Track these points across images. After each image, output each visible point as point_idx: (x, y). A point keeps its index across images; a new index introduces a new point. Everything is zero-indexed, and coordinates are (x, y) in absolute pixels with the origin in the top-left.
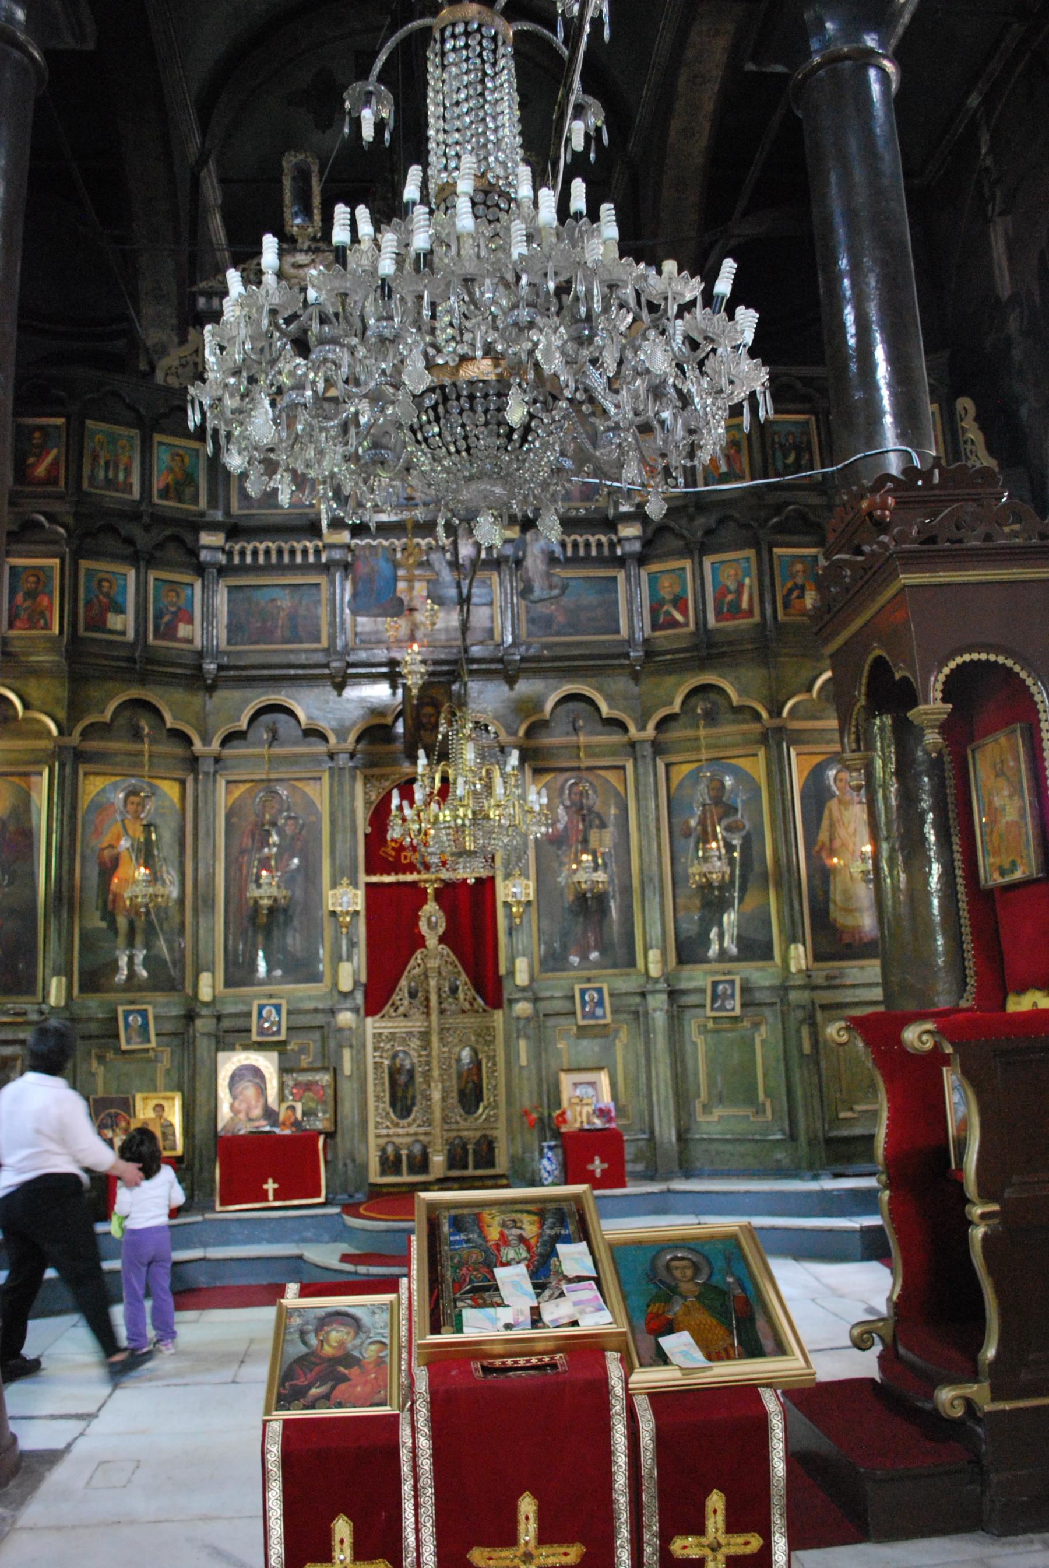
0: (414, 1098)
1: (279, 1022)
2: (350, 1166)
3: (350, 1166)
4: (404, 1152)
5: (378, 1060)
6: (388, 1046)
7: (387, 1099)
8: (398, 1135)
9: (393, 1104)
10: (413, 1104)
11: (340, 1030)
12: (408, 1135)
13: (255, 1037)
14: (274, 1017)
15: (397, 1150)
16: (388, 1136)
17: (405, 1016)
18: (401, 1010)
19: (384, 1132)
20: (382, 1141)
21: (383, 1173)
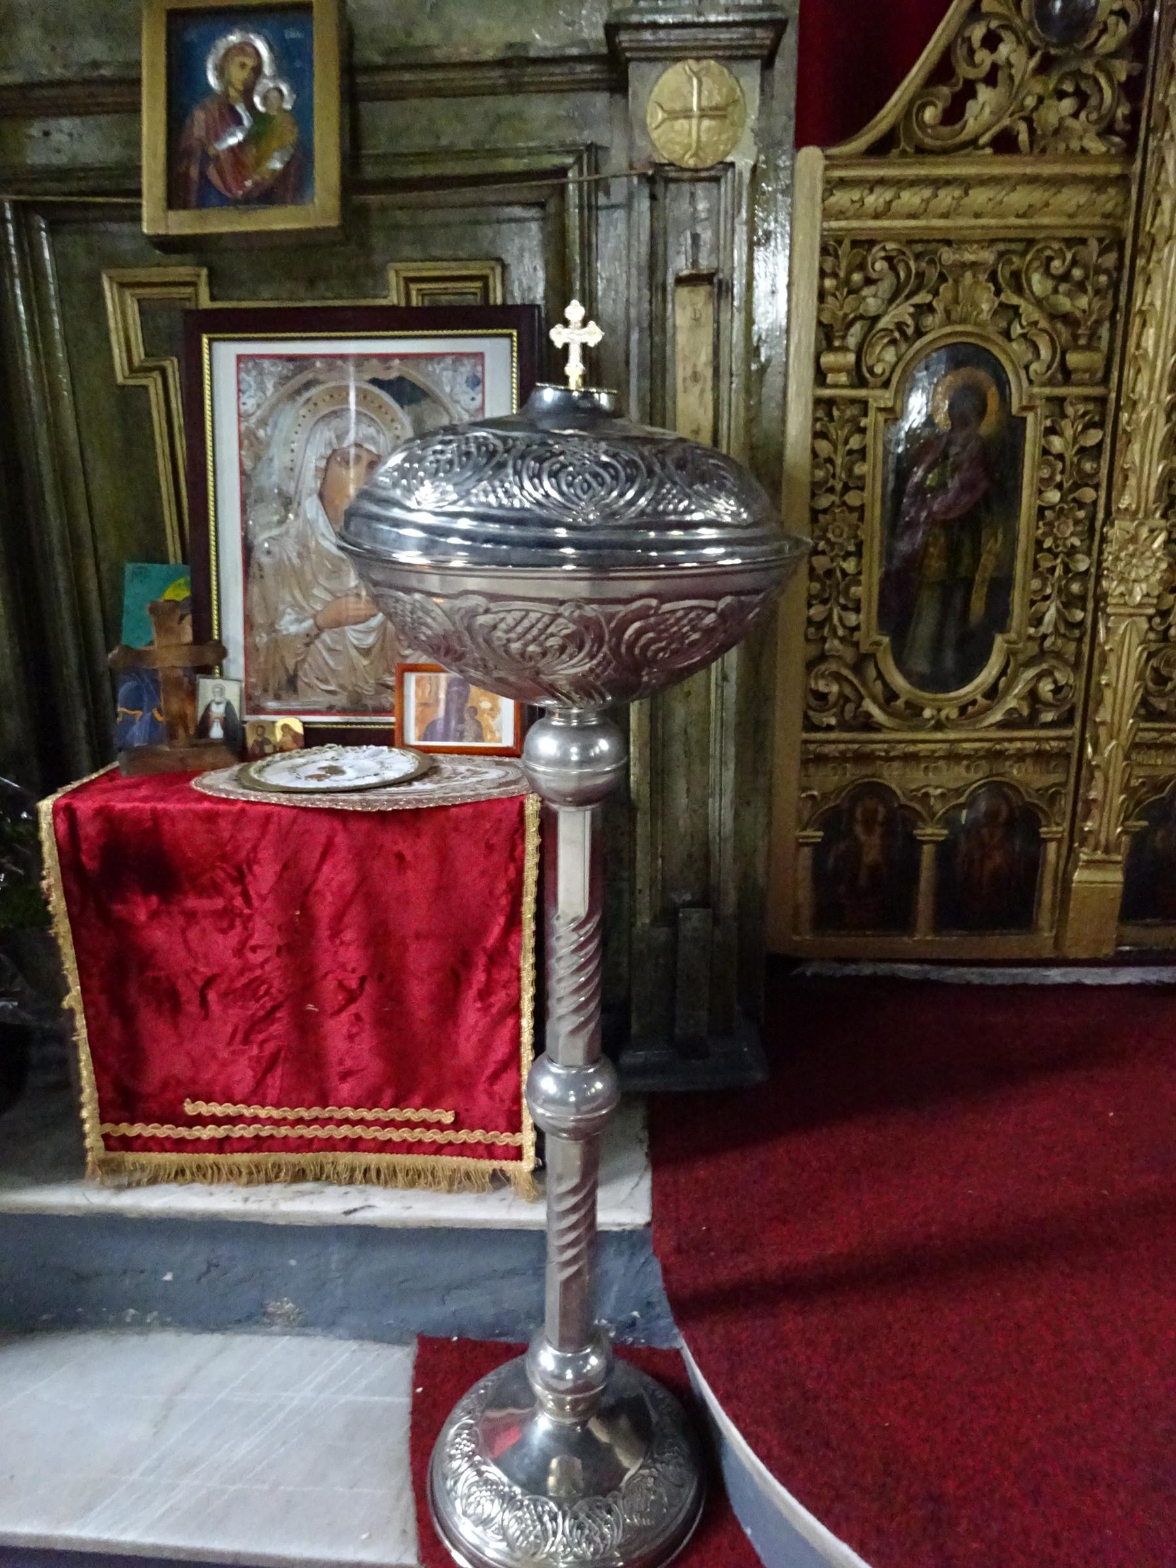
0: (1001, 586)
1: (303, 114)
2: (694, 921)
3: (694, 921)
4: (931, 832)
5: (840, 387)
6: (903, 311)
7: (867, 590)
8: (910, 758)
9: (896, 614)
10: (998, 618)
11: (659, 178)
12: (953, 757)
13: (154, 217)
14: (273, 91)
15: (899, 821)
16: (862, 758)
17: (1005, 143)
18: (984, 108)
19: (838, 741)
20: (828, 780)
21: (828, 915)
